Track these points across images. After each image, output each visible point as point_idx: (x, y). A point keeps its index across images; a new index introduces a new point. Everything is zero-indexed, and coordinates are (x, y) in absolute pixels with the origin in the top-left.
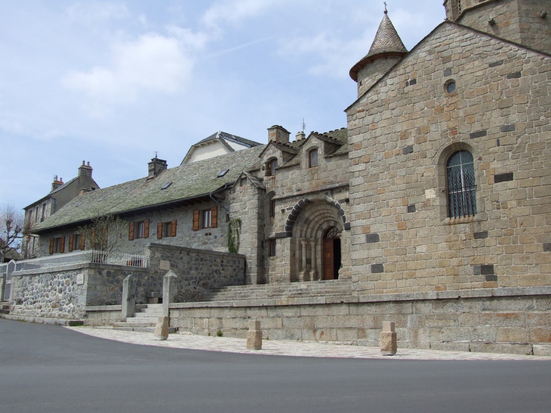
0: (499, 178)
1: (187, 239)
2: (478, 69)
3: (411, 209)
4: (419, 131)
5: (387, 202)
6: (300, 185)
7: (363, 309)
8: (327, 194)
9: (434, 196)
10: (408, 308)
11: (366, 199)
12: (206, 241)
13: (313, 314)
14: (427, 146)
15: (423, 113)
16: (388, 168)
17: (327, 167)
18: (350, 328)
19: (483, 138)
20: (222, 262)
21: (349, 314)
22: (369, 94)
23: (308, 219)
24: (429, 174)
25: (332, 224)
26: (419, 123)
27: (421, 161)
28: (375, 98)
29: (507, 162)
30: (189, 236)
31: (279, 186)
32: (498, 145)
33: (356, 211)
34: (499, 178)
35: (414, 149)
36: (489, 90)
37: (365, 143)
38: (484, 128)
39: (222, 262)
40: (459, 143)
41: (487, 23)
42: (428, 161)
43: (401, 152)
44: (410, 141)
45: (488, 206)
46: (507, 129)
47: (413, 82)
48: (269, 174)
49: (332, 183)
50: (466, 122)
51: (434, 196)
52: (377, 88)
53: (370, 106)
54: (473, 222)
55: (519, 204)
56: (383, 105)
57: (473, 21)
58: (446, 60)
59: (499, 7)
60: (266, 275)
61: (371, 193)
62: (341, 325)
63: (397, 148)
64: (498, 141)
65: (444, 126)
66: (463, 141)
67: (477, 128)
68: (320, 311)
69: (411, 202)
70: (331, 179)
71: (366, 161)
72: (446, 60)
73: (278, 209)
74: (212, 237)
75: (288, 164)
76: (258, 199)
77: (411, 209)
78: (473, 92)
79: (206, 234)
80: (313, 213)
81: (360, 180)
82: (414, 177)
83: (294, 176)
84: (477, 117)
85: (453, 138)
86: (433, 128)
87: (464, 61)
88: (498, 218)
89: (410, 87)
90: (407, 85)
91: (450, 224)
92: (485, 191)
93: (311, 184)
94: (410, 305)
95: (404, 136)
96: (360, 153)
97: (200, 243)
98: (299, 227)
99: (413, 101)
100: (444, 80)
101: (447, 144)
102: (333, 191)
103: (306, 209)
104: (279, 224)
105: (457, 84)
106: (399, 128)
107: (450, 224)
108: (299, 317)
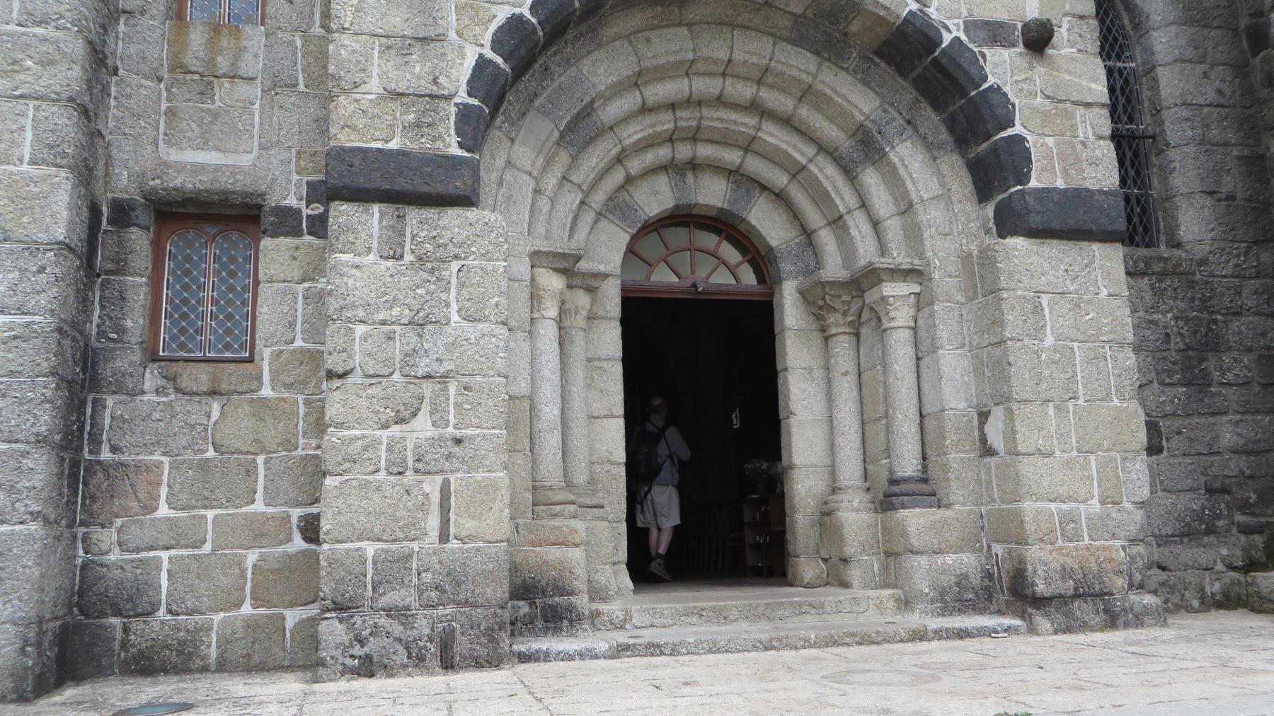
23: (587, 111)
25: (712, 193)
60: (106, 538)
80: (636, 82)
98: (524, 154)
103: (609, 32)
104: (379, 75)
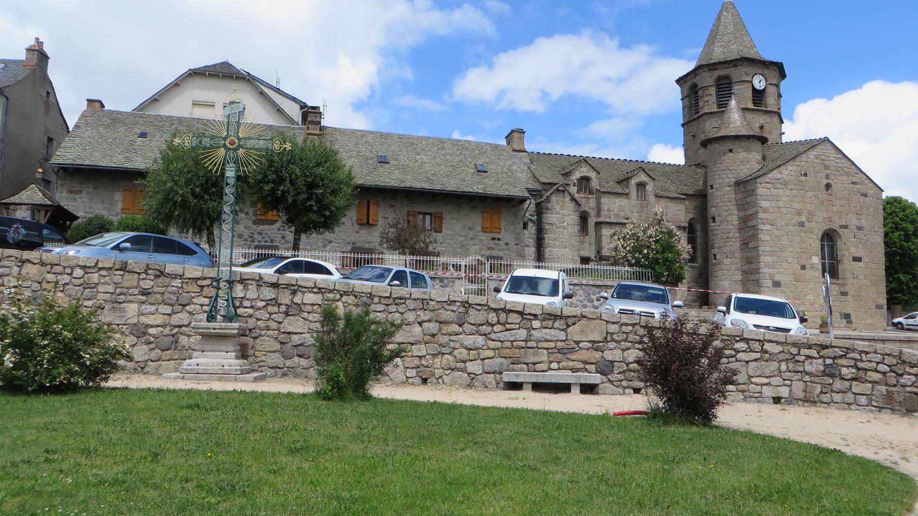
1: (462, 239)
4: (809, 212)
6: (629, 214)
11: (772, 253)
14: (813, 225)
22: (775, 172)
26: (810, 207)
27: (810, 235)
28: (779, 176)
30: (465, 236)
37: (771, 210)
41: (757, 125)
44: (803, 219)
46: (860, 228)
52: (780, 169)
53: (774, 181)
56: (785, 184)
61: (776, 249)
67: (844, 223)
79: (493, 239)
84: (844, 215)
86: (818, 213)
95: (799, 213)
97: (484, 247)
101: (827, 228)
106: (797, 206)
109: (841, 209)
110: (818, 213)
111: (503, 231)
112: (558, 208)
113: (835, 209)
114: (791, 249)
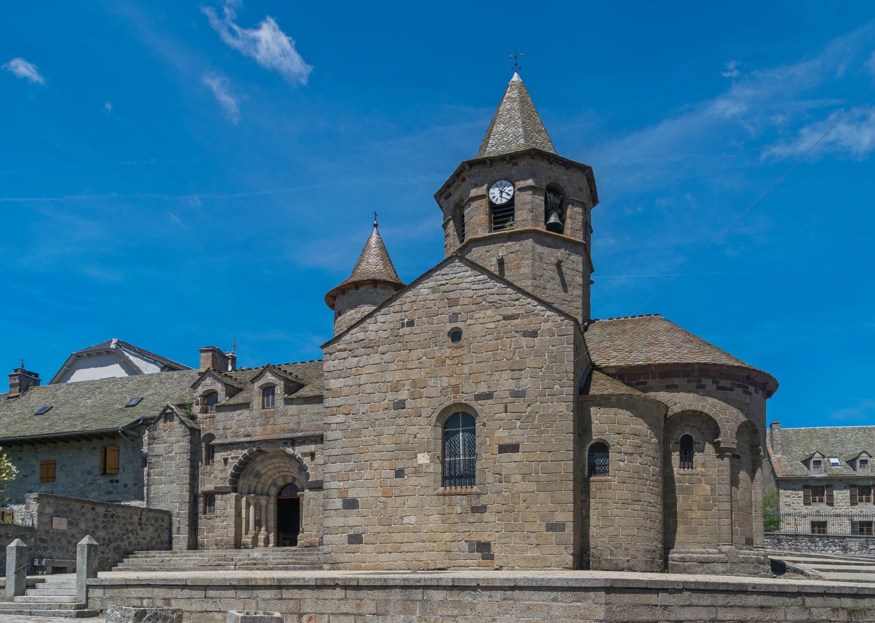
0: (504, 449)
2: (490, 320)
3: (399, 473)
4: (414, 383)
5: (371, 464)
6: (250, 430)
7: (362, 594)
8: (286, 444)
9: (428, 461)
10: (418, 594)
11: (345, 457)
12: (111, 490)
13: (298, 596)
14: (424, 402)
15: (420, 363)
16: (373, 425)
17: (286, 410)
18: (346, 614)
19: (489, 401)
20: (140, 519)
21: (346, 598)
24: (424, 436)
26: (414, 375)
27: (415, 420)
29: (514, 432)
31: (221, 427)
32: (506, 412)
33: (331, 470)
34: (504, 449)
35: (407, 405)
36: (500, 347)
38: (491, 390)
39: (140, 519)
40: (461, 404)
42: (423, 421)
43: (391, 406)
44: (403, 395)
45: (490, 478)
47: (411, 323)
48: (205, 411)
49: (293, 430)
50: (470, 381)
51: (428, 461)
54: (471, 494)
55: (524, 479)
57: (479, 255)
58: (453, 302)
59: (510, 243)
61: (351, 451)
62: (333, 610)
63: (386, 401)
64: (506, 407)
65: (445, 382)
66: (467, 402)
67: (483, 389)
68: (308, 594)
69: (400, 465)
70: (292, 426)
71: (346, 412)
72: (453, 302)
73: (219, 456)
74: (119, 484)
75: (233, 401)
76: (191, 442)
77: (399, 473)
78: (481, 346)
81: (338, 434)
82: (405, 438)
83: (242, 417)
84: (483, 377)
85: (455, 397)
87: (474, 307)
88: (499, 493)
89: (407, 329)
90: (403, 326)
91: (444, 495)
92: (487, 461)
93: (264, 429)
94: (420, 591)
95: (395, 389)
96: (339, 401)
99: (409, 347)
100: (449, 327)
101: (447, 404)
102: (293, 442)
105: (464, 336)
106: (389, 377)
107: (444, 495)
108: (281, 599)
109: (476, 367)
110: (431, 382)
111: (121, 470)
112: (165, 435)
113: (466, 369)
114: (379, 447)
